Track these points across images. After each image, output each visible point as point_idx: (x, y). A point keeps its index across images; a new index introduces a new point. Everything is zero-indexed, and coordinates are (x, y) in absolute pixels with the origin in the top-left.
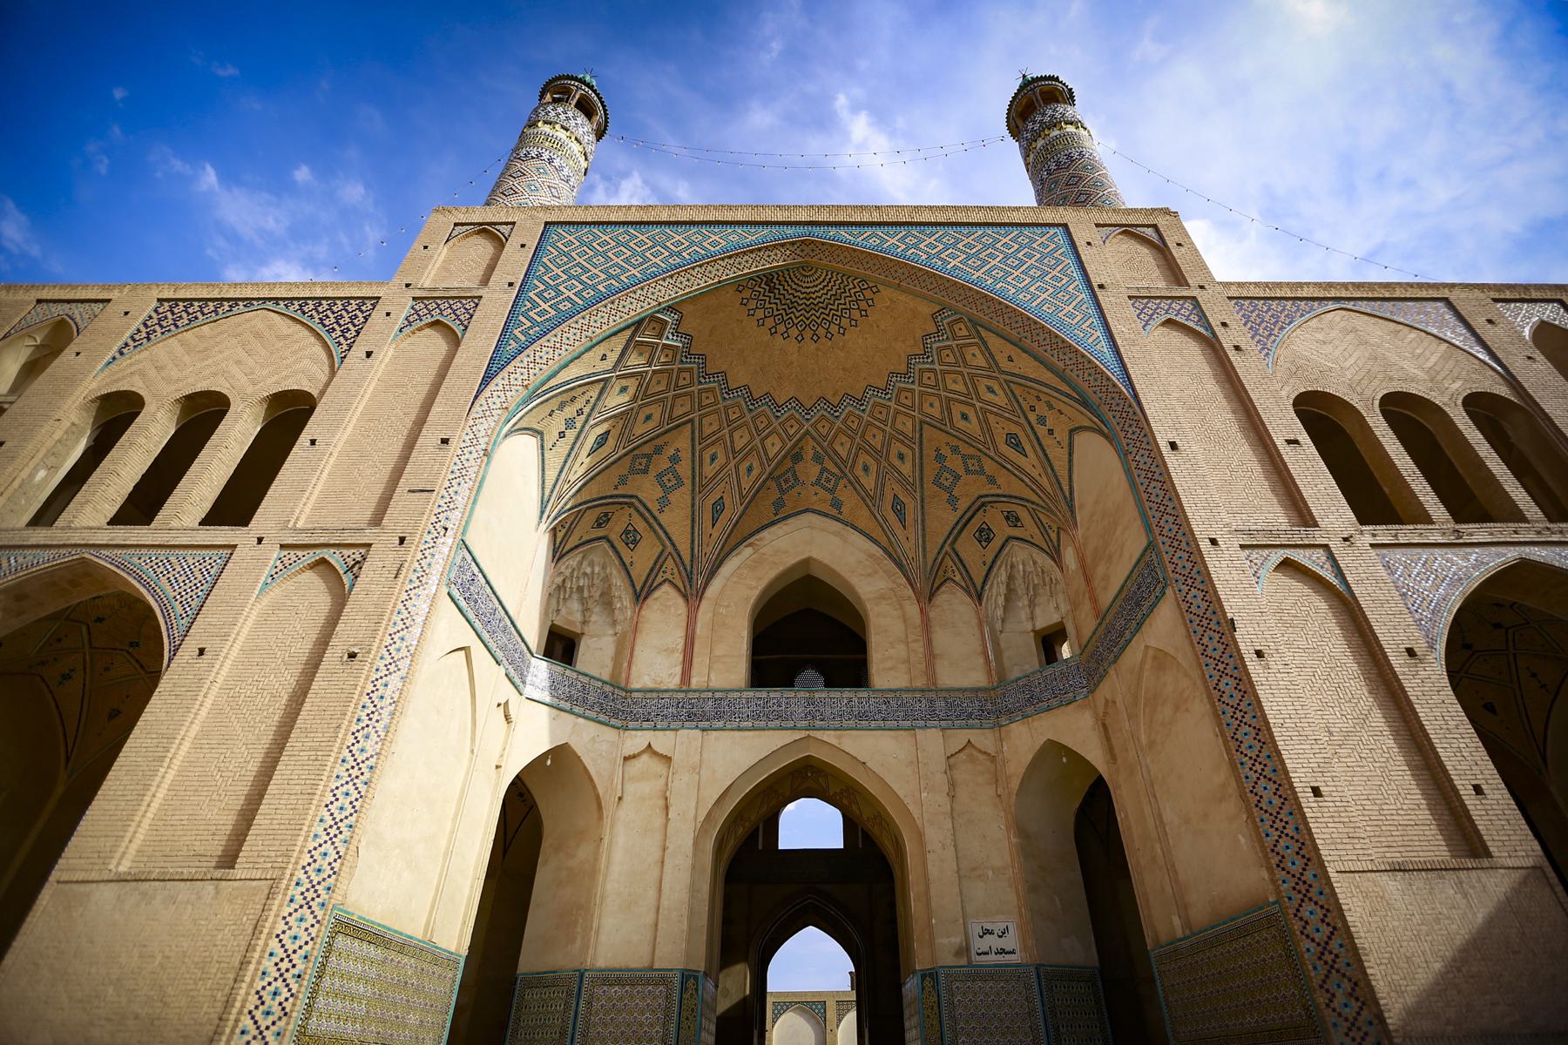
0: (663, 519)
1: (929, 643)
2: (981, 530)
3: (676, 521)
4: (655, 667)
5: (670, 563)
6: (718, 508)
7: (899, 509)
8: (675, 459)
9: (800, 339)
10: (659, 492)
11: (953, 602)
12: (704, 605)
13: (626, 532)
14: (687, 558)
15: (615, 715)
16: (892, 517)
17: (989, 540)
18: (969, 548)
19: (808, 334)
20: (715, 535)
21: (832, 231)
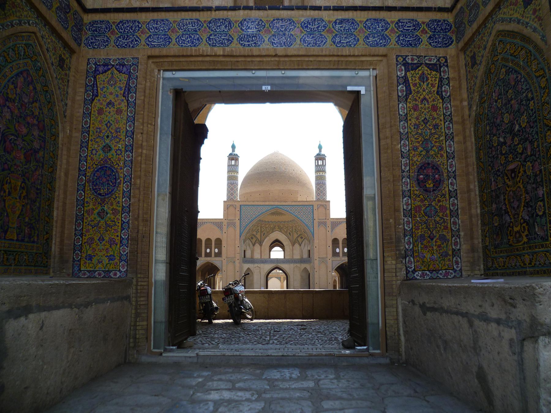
4: (257, 256)
6: (264, 234)
11: (297, 245)
18: (299, 239)
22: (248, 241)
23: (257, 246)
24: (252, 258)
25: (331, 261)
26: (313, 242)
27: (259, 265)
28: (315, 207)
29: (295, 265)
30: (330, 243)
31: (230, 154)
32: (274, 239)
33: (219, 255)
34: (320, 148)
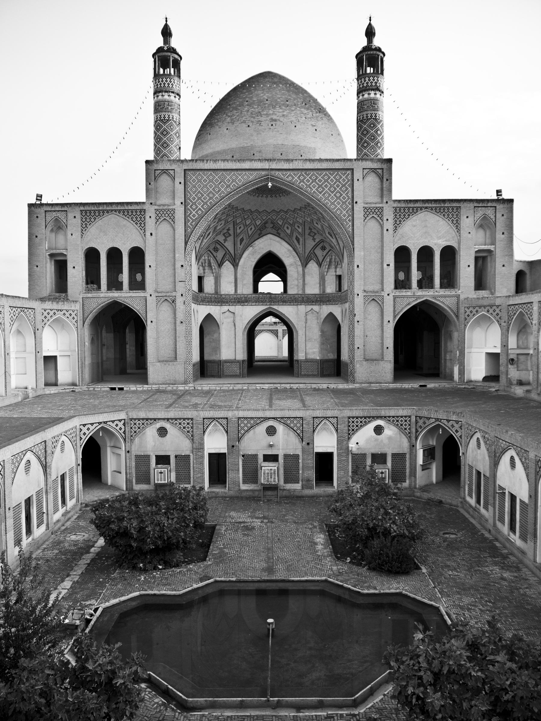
0: (226, 244)
1: (304, 281)
2: (322, 247)
3: (229, 244)
4: (227, 288)
6: (242, 240)
7: (298, 240)
8: (228, 230)
9: (267, 197)
10: (224, 238)
11: (313, 266)
13: (214, 248)
16: (295, 241)
17: (325, 250)
18: (319, 252)
19: (269, 196)
20: (241, 247)
21: (277, 173)
23: (227, 265)
24: (216, 293)
25: (391, 296)
26: (351, 255)
27: (232, 308)
28: (358, 174)
29: (309, 307)
30: (390, 258)
31: (160, 50)
32: (264, 251)
33: (138, 285)
34: (370, 33)
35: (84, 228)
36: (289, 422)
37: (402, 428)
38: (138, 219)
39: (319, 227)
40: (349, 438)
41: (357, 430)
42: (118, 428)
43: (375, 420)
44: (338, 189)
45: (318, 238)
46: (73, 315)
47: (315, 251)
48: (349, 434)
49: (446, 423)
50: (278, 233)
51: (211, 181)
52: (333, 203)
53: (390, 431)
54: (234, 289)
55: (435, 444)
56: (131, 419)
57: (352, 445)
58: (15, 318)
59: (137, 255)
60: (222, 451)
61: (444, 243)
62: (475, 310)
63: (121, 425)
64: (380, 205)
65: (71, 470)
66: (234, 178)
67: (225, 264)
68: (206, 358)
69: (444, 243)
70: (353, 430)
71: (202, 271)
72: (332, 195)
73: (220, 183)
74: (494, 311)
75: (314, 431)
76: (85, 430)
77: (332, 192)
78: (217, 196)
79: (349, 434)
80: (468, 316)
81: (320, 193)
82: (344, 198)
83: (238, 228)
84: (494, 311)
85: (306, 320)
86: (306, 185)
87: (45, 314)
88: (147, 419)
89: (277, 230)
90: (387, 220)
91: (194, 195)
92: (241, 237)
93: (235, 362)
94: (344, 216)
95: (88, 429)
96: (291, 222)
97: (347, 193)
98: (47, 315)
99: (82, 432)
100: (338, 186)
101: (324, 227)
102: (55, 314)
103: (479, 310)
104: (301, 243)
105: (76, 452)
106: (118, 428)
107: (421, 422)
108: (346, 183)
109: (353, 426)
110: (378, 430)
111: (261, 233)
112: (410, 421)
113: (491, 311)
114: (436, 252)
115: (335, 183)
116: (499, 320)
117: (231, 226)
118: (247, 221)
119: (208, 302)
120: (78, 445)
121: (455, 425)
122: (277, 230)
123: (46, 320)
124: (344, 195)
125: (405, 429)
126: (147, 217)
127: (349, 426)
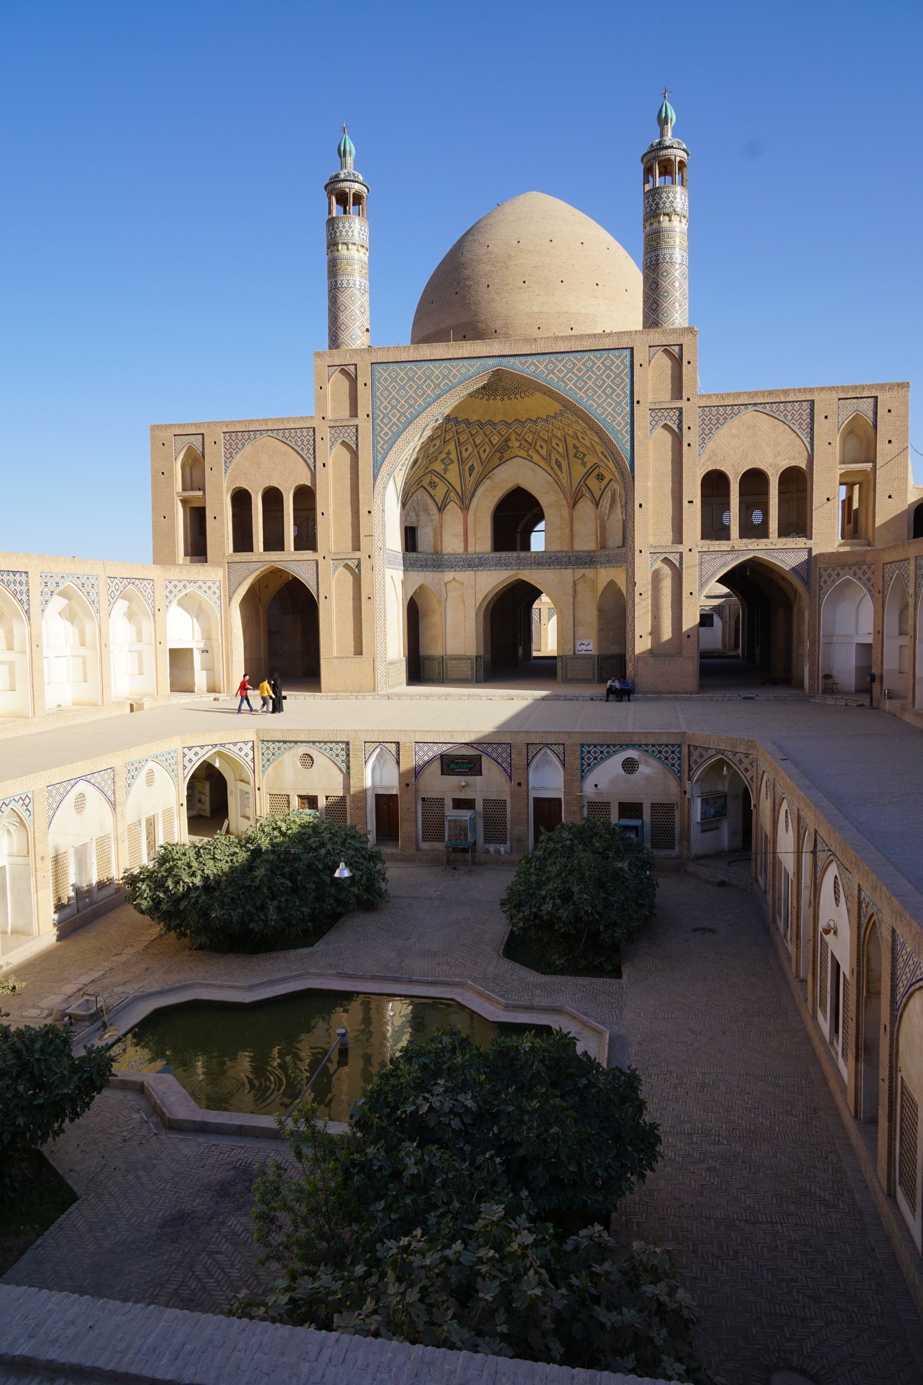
0: (445, 476)
1: (572, 530)
2: (598, 475)
3: (453, 475)
4: (452, 545)
5: (452, 494)
6: (472, 469)
7: (559, 465)
8: (448, 453)
10: (443, 466)
11: (585, 507)
12: (471, 512)
13: (430, 483)
14: (460, 492)
15: (439, 567)
16: (556, 468)
17: (602, 479)
18: (592, 482)
19: (506, 398)
22: (421, 495)
23: (453, 509)
29: (580, 572)
30: (693, 490)
31: (336, 180)
33: (307, 540)
35: (229, 457)
36: (490, 750)
37: (667, 764)
38: (305, 443)
39: (587, 443)
40: (582, 777)
41: (595, 764)
42: (242, 754)
43: (624, 750)
44: (609, 382)
45: (591, 460)
46: (214, 588)
47: (588, 482)
48: (583, 771)
49: (731, 757)
50: (529, 455)
51: (411, 379)
52: (600, 405)
53: (648, 768)
54: (462, 545)
55: (726, 789)
56: (263, 741)
57: (588, 789)
58: (117, 593)
59: (306, 497)
60: (395, 793)
61: (784, 462)
62: (836, 572)
63: (247, 749)
64: (678, 404)
65: (168, 812)
66: (446, 372)
67: (448, 507)
68: (423, 652)
69: (785, 464)
70: (589, 765)
71: (415, 518)
72: (599, 392)
73: (425, 381)
74: (864, 573)
75: (528, 765)
76: (190, 755)
77: (600, 388)
78: (420, 401)
79: (583, 771)
80: (825, 582)
81: (580, 389)
82: (618, 395)
83: (463, 450)
84: (864, 573)
85: (575, 592)
86: (558, 377)
87: (171, 587)
88: (285, 742)
89: (527, 451)
90: (689, 428)
91: (386, 403)
92: (469, 464)
93: (464, 659)
94: (619, 424)
95: (196, 754)
96: (546, 437)
97: (623, 388)
98: (173, 589)
99: (187, 758)
100: (608, 377)
101: (594, 443)
102: (185, 586)
103: (842, 573)
104: (564, 470)
105: (177, 786)
106: (242, 754)
107: (695, 754)
108: (622, 371)
109: (589, 759)
110: (630, 766)
111: (502, 453)
112: (680, 752)
113: (860, 574)
114: (771, 478)
115: (604, 372)
116: (871, 589)
117: (451, 447)
118: (476, 439)
119: (421, 566)
120: (181, 776)
121: (744, 760)
122: (527, 451)
123: (171, 597)
124: (618, 391)
125: (673, 765)
126: (318, 439)
127: (583, 758)
